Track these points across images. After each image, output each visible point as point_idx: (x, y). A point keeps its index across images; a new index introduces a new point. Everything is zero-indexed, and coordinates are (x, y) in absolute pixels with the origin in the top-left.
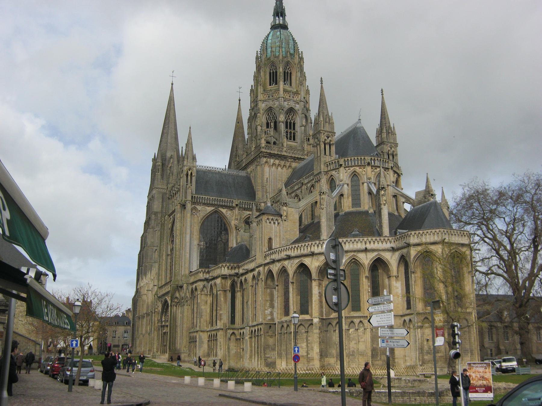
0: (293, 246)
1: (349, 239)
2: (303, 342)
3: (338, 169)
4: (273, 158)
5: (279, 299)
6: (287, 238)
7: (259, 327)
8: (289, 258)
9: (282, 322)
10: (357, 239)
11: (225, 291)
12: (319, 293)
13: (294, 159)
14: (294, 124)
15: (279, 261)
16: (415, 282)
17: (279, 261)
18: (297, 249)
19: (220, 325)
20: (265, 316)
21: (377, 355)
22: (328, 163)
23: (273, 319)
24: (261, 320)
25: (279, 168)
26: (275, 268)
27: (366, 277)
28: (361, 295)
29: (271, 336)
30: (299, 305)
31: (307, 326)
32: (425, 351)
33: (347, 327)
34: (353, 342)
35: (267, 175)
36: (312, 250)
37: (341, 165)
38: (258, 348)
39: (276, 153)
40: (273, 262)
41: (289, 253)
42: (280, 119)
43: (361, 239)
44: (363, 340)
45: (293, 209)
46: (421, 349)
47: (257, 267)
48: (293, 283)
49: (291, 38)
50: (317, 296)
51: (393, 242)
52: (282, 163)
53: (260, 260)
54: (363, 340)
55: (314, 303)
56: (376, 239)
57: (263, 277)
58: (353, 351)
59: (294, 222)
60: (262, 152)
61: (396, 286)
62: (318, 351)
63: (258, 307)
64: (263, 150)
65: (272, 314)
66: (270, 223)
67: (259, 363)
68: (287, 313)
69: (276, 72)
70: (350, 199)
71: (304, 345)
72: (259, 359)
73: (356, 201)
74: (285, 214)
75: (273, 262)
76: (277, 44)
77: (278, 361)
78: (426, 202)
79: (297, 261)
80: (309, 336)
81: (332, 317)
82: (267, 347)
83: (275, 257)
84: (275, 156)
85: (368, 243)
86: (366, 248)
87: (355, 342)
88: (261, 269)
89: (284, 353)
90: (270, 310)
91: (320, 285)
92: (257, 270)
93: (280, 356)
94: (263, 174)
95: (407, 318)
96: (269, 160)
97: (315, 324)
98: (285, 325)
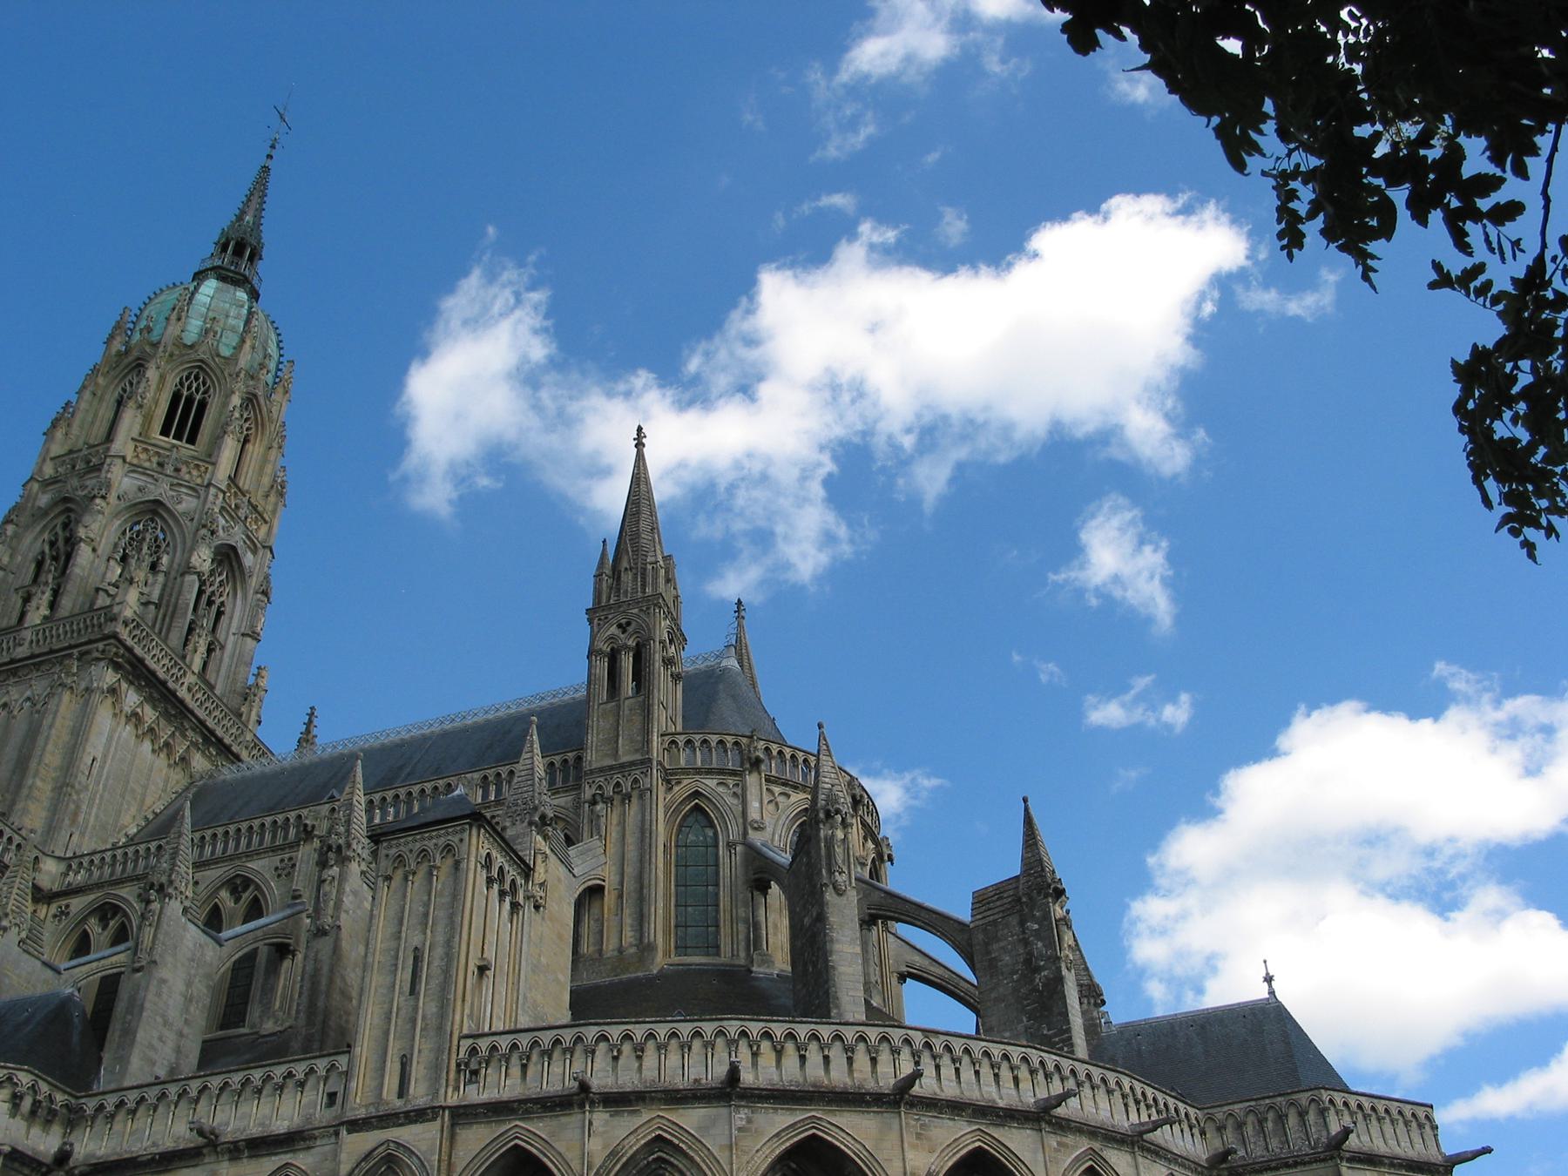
3: (733, 773)
4: (139, 689)
13: (205, 739)
14: (219, 614)
15: (618, 1101)
17: (618, 1101)
18: (779, 1053)
22: (681, 740)
25: (147, 746)
35: (95, 746)
37: (756, 764)
39: (161, 674)
40: (580, 1097)
42: (195, 560)
47: (355, 1126)
49: (273, 337)
52: (166, 732)
60: (115, 636)
64: (124, 634)
69: (203, 405)
76: (231, 321)
84: (149, 684)
88: (421, 1138)
94: (79, 733)
96: (124, 685)
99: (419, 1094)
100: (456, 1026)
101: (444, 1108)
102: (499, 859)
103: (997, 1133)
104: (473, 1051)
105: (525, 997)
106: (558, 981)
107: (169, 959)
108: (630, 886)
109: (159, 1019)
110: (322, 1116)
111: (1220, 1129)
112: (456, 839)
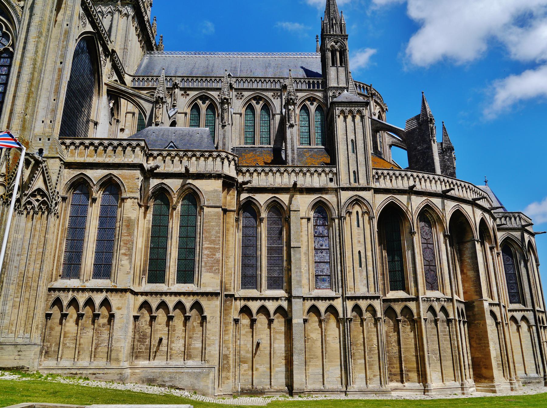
11: (225, 211)
19: (208, 281)
47: (344, 189)
99: (363, 182)
101: (372, 188)
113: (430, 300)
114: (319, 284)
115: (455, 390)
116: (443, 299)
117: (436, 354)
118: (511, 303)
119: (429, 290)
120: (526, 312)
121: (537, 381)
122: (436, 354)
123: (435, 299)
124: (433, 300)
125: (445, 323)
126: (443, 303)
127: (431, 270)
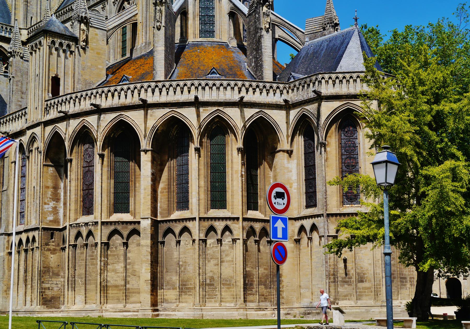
0: (106, 89)
1: (211, 83)
2: (118, 262)
5: (73, 183)
6: (85, 80)
7: (31, 235)
8: (98, 111)
9: (78, 225)
10: (225, 83)
12: (153, 174)
15: (76, 116)
16: (326, 160)
17: (76, 116)
18: (113, 96)
20: (42, 214)
21: (252, 284)
23: (56, 221)
24: (33, 223)
26: (68, 130)
27: (239, 150)
28: (229, 179)
29: (53, 252)
30: (112, 196)
31: (125, 234)
32: (340, 279)
33: (202, 236)
34: (213, 262)
36: (143, 96)
38: (26, 271)
41: (98, 101)
43: (232, 83)
44: (229, 258)
45: (97, 30)
46: (334, 275)
47: (29, 128)
48: (102, 156)
50: (150, 179)
51: (285, 91)
53: (35, 115)
54: (229, 258)
55: (142, 191)
56: (258, 86)
57: (40, 144)
58: (212, 278)
59: (98, 53)
61: (288, 168)
62: (148, 276)
63: (29, 199)
65: (55, 211)
66: (57, 49)
67: (28, 298)
68: (87, 208)
70: (197, 22)
71: (120, 266)
72: (29, 291)
73: (207, 28)
74: (83, 37)
75: (66, 117)
77: (69, 294)
78: (325, 35)
79: (111, 116)
80: (130, 252)
81: (173, 217)
82: (46, 271)
83: (71, 109)
85: (243, 89)
86: (242, 98)
87: (216, 262)
88: (37, 130)
89: (80, 281)
90: (52, 204)
91: (153, 160)
92: (29, 133)
93: (73, 285)
95: (307, 224)
97: (145, 229)
98: (84, 234)
100: (43, 98)
102: (58, 41)
103: (179, 110)
104: (47, 105)
105: (79, 79)
106: (98, 68)
107: (19, 74)
108: (144, 21)
109: (19, 93)
110: (26, 126)
111: (293, 90)
112: (41, 38)
113: (79, 226)
114: (22, 220)
115: (89, 313)
116: (91, 224)
117: (82, 278)
118: (308, 206)
119: (86, 215)
120: (316, 218)
121: (317, 311)
122: (82, 278)
123: (83, 224)
124: (82, 226)
125: (94, 248)
126: (90, 227)
127: (90, 194)
